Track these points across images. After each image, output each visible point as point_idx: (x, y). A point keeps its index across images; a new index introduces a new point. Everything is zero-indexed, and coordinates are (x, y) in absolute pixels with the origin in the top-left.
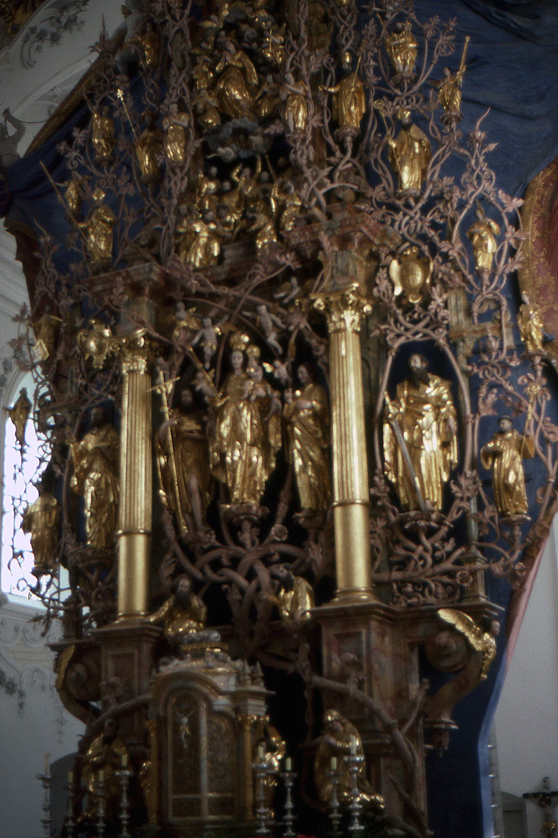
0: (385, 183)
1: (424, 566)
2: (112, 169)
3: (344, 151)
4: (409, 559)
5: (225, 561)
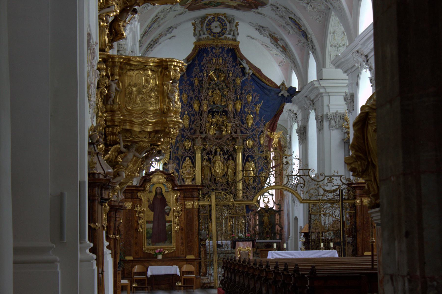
3: (237, 115)
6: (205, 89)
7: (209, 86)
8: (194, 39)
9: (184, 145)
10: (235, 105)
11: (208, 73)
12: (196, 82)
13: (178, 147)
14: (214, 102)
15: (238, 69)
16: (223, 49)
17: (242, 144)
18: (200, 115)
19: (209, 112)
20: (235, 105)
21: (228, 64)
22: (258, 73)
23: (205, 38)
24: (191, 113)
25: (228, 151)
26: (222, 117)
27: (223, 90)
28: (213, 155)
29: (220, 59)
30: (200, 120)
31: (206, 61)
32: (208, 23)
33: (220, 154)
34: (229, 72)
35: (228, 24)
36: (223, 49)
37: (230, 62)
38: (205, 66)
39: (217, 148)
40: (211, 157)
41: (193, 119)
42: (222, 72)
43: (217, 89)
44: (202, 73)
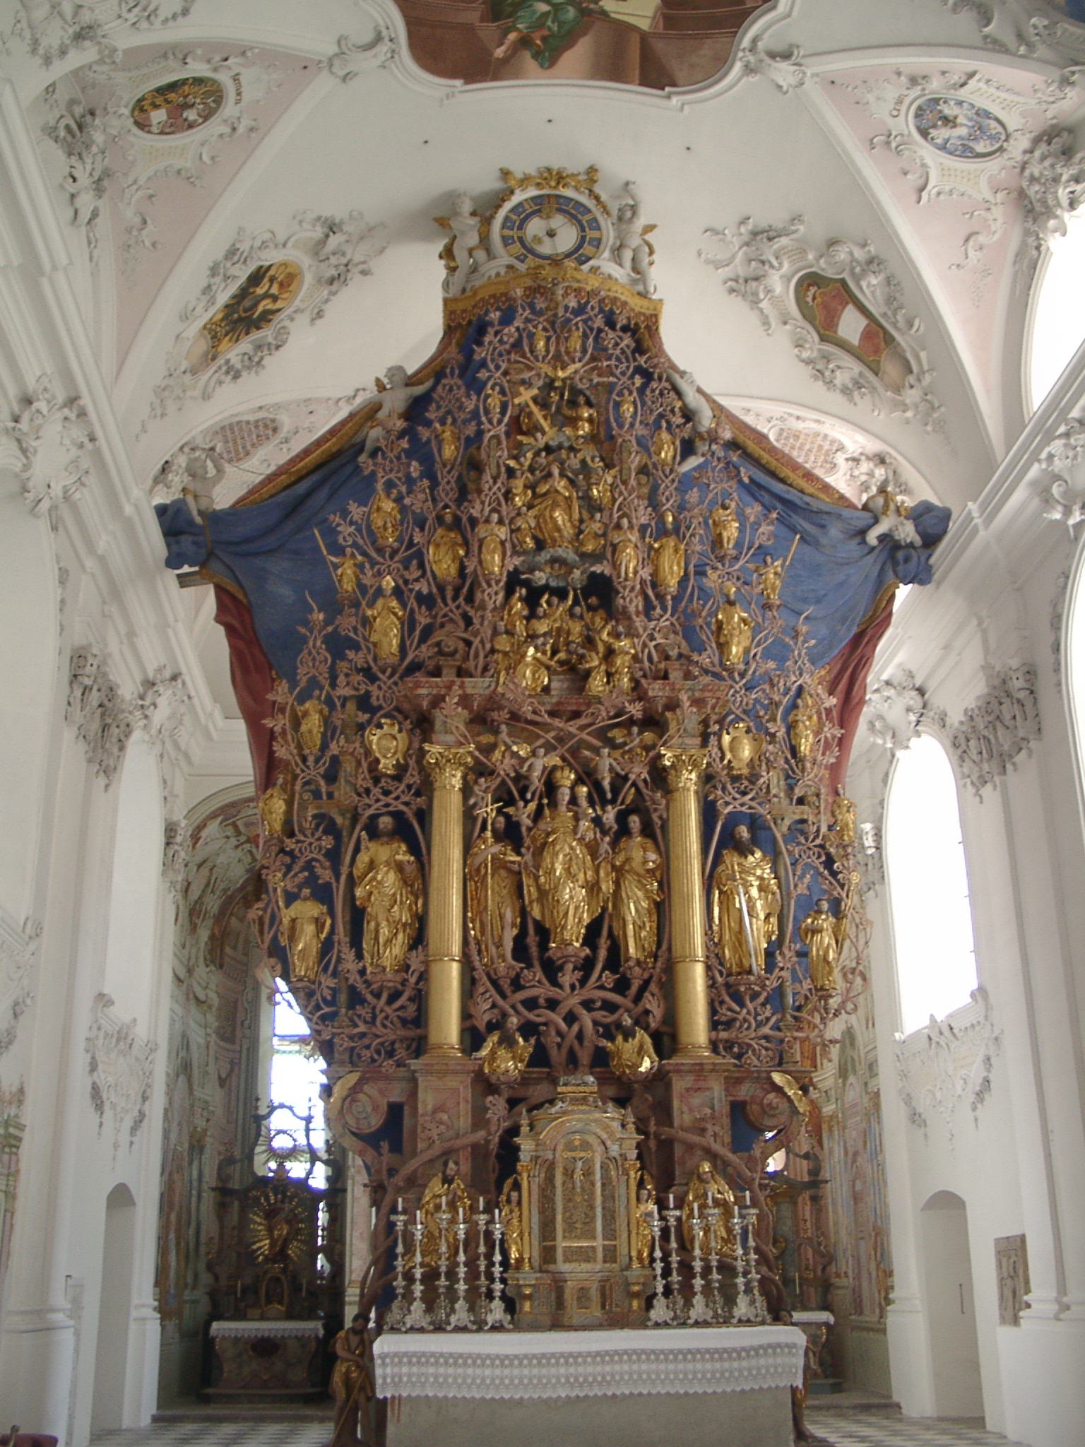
0: (709, 651)
1: (748, 1028)
2: (396, 559)
3: (664, 609)
4: (734, 1020)
5: (542, 1001)
6: (494, 471)
7: (516, 458)
9: (368, 752)
10: (652, 556)
13: (335, 761)
14: (540, 545)
15: (661, 394)
17: (698, 741)
18: (461, 600)
19: (514, 581)
20: (652, 556)
21: (613, 362)
22: (759, 443)
23: (498, 274)
24: (417, 587)
25: (619, 781)
26: (581, 617)
27: (587, 478)
28: (532, 806)
29: (567, 339)
30: (462, 624)
31: (501, 341)
32: (514, 217)
33: (574, 800)
34: (620, 394)
37: (623, 352)
38: (492, 367)
39: (555, 768)
40: (524, 813)
41: (423, 619)
42: (581, 400)
43: (556, 472)
44: (479, 395)
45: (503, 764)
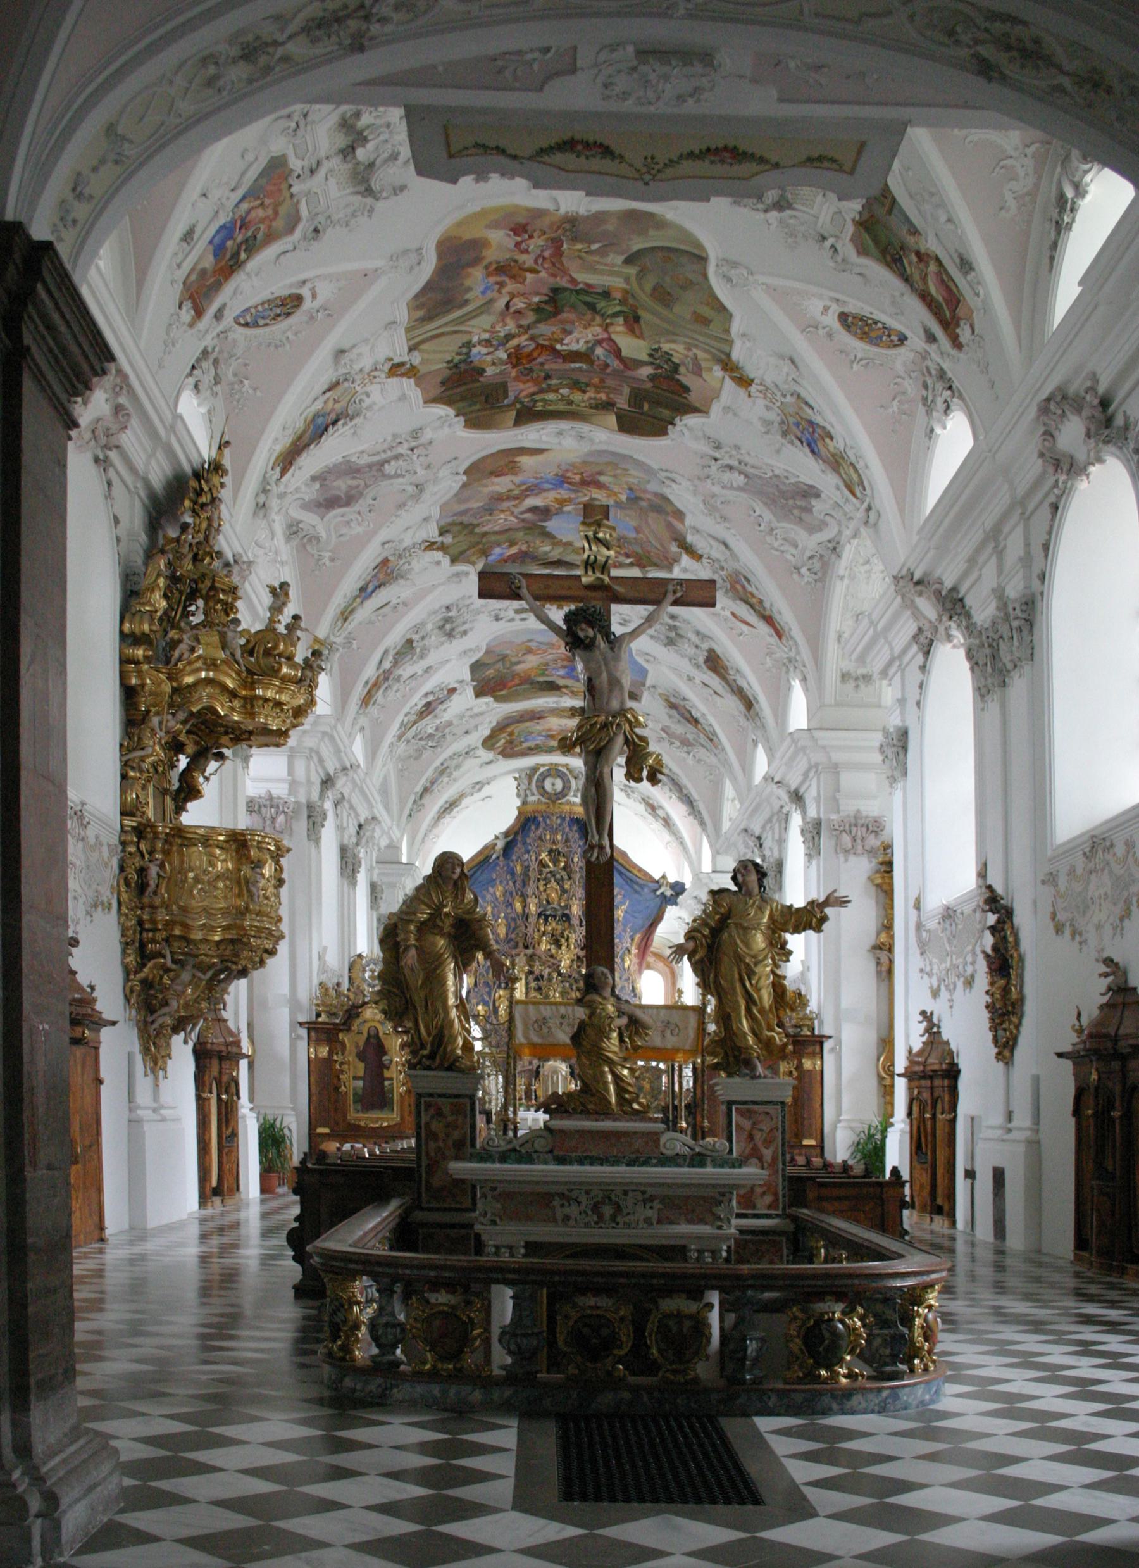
8: (518, 803)
11: (538, 854)
12: (519, 869)
16: (563, 819)
19: (540, 915)
35: (573, 781)
36: (563, 819)
45: (537, 972)
